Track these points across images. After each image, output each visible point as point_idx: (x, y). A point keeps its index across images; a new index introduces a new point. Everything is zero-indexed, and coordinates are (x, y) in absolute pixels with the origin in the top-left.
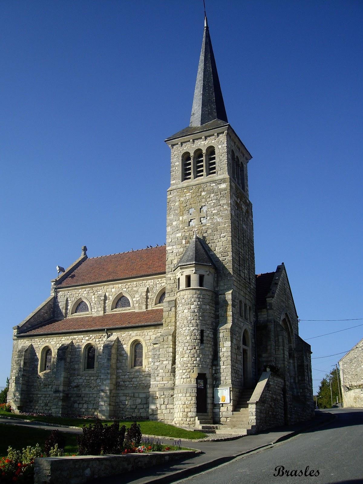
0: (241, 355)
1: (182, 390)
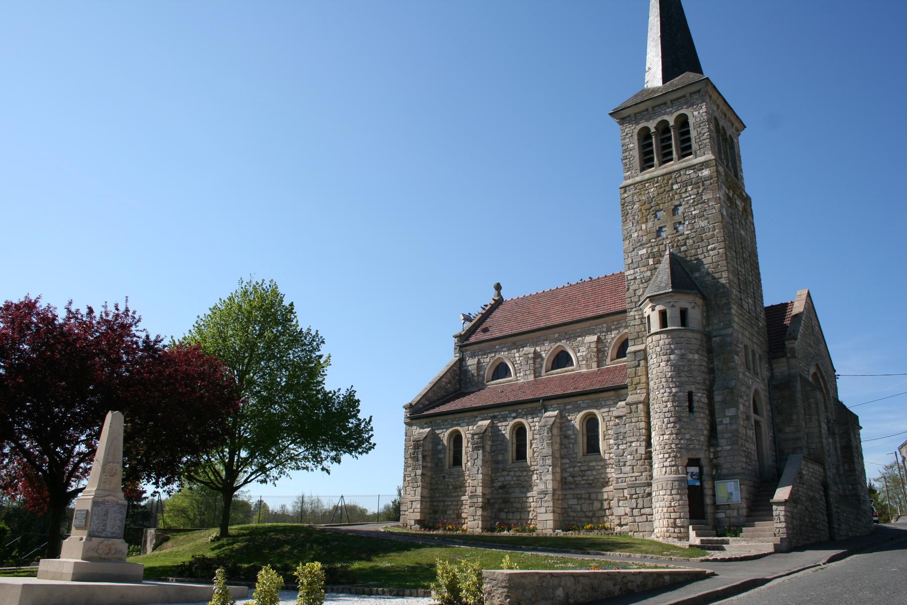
0: (752, 429)
1: (664, 485)
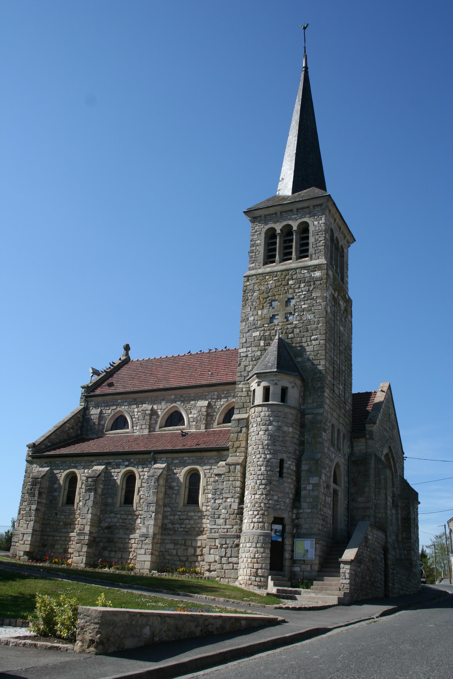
0: (331, 497)
1: (251, 539)
